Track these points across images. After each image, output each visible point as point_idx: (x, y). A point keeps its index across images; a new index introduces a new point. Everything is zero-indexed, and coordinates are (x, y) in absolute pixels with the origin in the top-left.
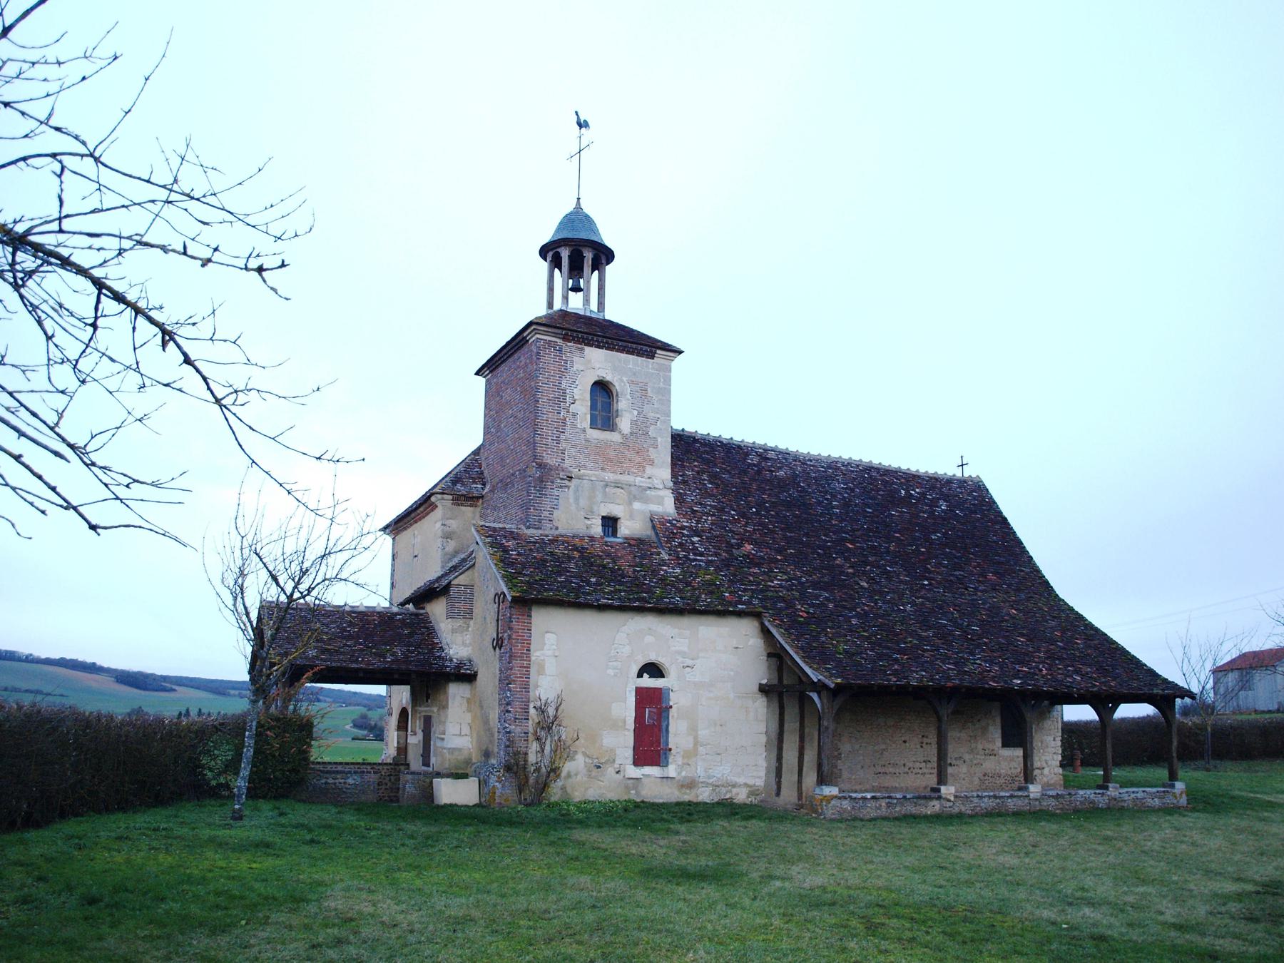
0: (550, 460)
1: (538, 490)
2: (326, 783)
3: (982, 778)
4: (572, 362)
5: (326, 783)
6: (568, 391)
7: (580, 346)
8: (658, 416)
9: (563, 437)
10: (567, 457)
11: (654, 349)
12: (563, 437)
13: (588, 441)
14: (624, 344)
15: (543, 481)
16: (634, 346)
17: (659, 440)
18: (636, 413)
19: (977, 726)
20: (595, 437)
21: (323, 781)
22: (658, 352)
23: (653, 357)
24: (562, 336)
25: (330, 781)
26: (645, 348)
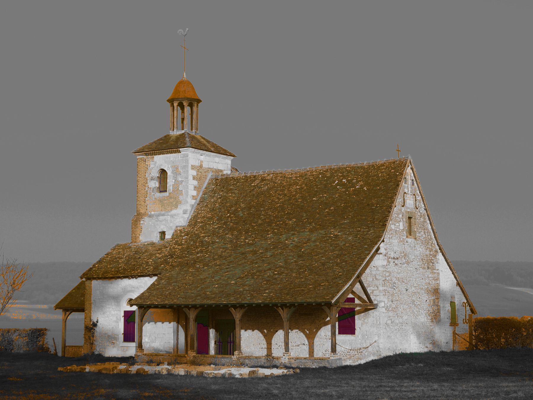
0: (142, 211)
1: (135, 226)
2: (74, 351)
3: (324, 352)
4: (149, 165)
5: (74, 351)
6: (148, 178)
7: (152, 156)
8: (183, 179)
9: (146, 199)
10: (148, 208)
11: (178, 149)
12: (146, 199)
13: (155, 199)
14: (167, 150)
15: (137, 221)
16: (171, 150)
17: (183, 191)
18: (174, 181)
19: (321, 322)
20: (158, 196)
21: (74, 350)
22: (180, 149)
23: (180, 152)
24: (145, 155)
25: (76, 350)
26: (174, 150)
